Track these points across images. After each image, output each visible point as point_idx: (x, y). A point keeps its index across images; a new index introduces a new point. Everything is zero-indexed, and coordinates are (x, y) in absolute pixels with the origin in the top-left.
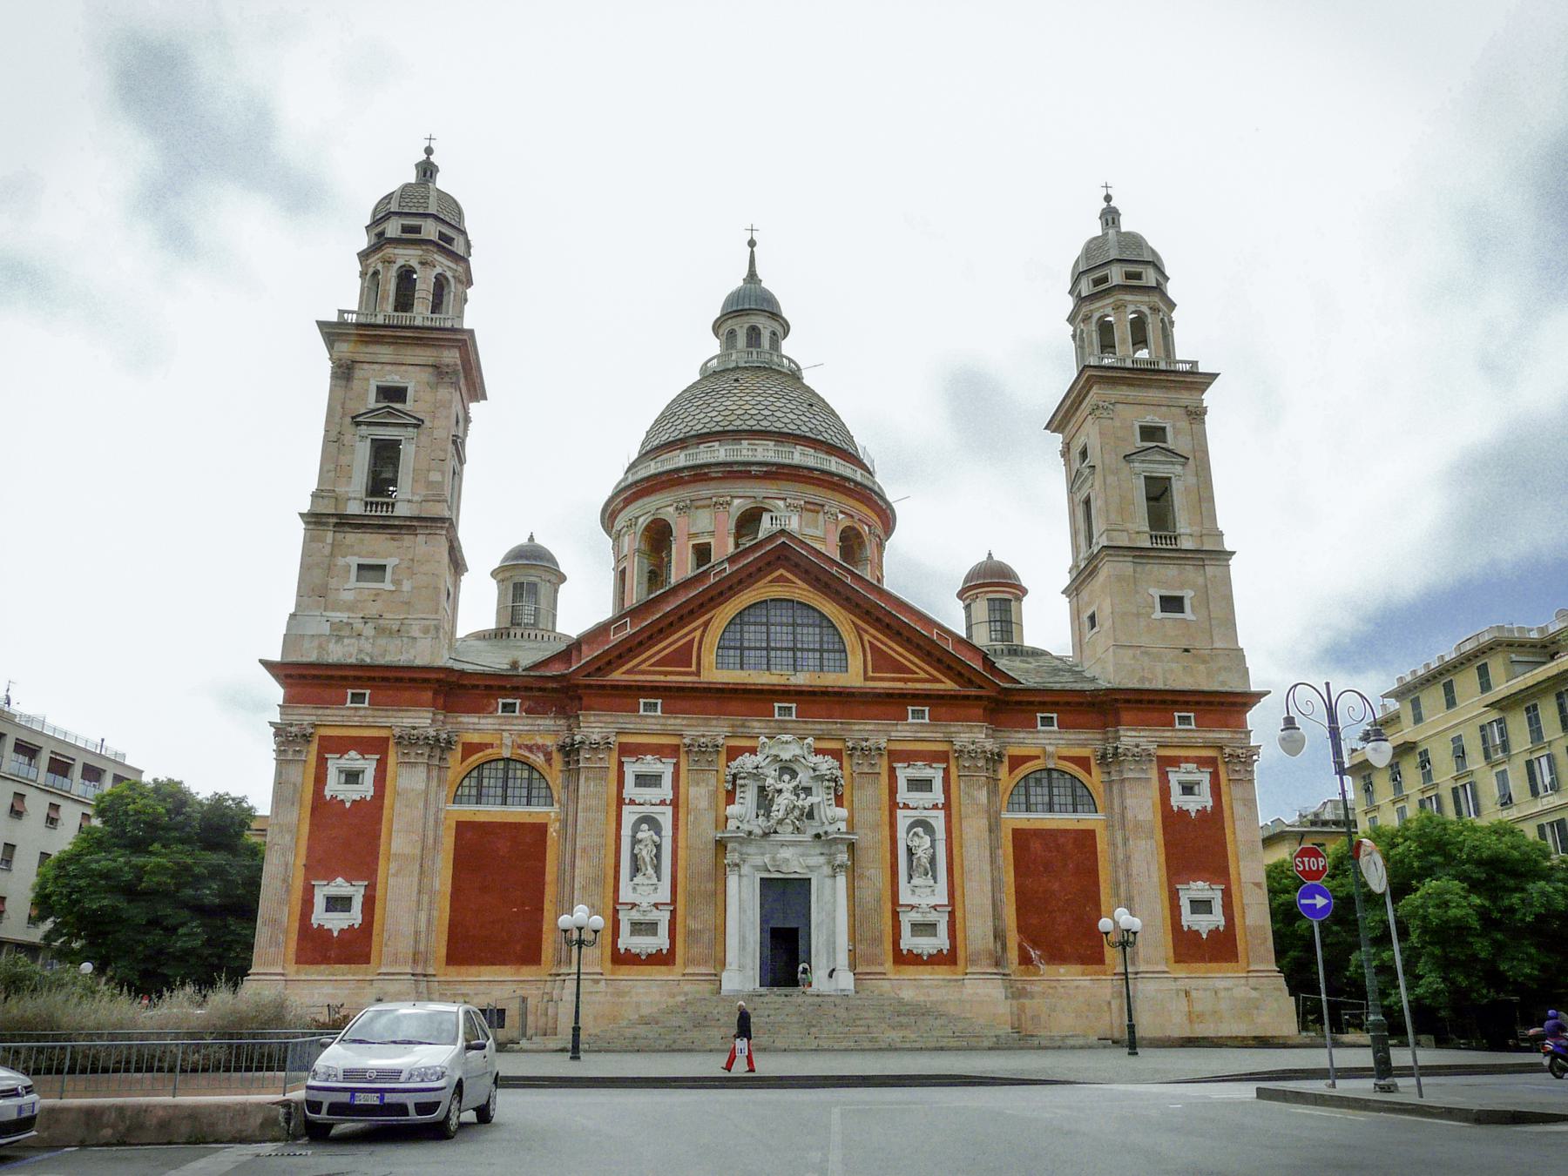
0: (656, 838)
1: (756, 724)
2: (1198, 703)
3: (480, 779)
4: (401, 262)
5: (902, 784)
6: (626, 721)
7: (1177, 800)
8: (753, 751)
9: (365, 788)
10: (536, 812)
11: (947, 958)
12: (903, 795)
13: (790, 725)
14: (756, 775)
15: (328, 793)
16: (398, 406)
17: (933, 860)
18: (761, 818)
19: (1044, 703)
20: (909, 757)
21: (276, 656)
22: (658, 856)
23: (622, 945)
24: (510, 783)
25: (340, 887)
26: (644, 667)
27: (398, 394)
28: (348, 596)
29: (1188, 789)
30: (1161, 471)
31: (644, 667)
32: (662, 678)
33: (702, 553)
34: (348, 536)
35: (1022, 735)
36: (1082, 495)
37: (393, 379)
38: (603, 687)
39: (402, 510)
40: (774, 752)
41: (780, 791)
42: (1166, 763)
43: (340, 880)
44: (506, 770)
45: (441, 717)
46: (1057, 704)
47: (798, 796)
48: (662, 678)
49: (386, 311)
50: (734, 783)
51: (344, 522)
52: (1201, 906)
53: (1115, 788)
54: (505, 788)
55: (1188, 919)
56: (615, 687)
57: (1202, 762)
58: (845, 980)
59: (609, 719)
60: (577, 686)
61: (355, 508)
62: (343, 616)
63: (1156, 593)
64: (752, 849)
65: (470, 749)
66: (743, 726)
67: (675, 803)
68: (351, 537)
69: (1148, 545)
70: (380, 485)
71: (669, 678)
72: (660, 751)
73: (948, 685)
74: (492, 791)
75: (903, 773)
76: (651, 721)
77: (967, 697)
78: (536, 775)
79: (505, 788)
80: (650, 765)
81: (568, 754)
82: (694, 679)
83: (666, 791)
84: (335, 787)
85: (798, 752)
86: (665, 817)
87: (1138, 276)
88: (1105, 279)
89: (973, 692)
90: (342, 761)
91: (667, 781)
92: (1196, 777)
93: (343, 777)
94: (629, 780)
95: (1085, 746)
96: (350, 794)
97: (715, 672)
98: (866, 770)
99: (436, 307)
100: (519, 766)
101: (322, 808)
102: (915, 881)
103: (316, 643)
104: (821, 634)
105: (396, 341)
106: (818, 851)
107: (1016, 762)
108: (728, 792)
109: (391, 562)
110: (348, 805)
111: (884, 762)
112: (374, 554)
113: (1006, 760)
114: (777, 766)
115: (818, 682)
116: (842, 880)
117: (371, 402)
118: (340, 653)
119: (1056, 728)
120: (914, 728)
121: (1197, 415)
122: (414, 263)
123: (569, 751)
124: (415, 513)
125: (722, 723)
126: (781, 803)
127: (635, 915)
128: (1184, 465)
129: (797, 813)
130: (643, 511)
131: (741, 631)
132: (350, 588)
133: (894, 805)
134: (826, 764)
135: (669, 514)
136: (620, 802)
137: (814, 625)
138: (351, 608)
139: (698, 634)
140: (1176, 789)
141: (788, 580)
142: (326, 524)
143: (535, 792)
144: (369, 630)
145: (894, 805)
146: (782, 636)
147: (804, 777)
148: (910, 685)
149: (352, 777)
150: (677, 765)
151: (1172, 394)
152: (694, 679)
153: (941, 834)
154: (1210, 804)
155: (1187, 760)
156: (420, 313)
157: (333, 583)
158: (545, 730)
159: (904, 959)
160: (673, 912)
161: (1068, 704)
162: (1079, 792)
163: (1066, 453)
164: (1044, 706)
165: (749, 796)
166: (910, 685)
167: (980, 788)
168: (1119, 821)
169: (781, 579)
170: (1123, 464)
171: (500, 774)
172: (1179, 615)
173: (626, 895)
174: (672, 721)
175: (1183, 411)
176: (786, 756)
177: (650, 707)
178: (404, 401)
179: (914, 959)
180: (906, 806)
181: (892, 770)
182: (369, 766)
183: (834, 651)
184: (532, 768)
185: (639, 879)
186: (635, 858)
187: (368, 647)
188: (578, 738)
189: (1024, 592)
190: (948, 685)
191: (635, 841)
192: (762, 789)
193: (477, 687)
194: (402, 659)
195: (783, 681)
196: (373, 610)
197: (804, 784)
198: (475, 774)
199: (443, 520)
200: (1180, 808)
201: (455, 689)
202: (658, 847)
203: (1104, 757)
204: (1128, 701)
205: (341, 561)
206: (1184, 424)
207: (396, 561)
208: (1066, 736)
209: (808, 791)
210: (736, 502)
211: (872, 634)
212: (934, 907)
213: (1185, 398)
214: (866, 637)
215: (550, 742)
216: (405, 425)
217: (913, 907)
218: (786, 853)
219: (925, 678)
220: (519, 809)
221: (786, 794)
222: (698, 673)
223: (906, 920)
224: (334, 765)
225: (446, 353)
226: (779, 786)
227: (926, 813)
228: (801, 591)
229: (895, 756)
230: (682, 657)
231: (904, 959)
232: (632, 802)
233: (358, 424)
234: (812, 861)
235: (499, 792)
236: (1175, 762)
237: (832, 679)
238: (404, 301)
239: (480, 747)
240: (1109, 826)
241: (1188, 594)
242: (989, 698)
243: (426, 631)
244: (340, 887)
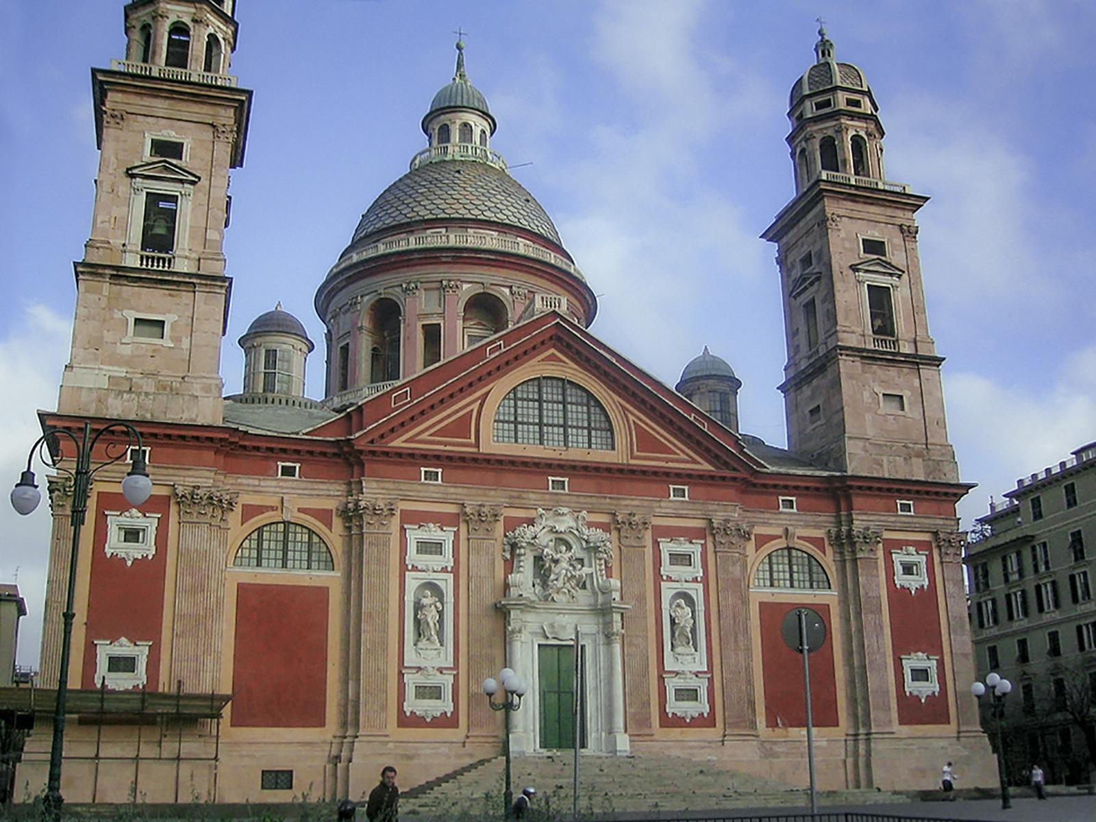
0: (438, 604)
1: (532, 496)
2: (918, 492)
3: (260, 540)
4: (173, 18)
5: (665, 557)
6: (407, 487)
7: (901, 579)
8: (531, 522)
9: (146, 549)
10: (318, 577)
11: (706, 721)
12: (666, 569)
13: (564, 498)
15: (108, 551)
16: (174, 161)
17: (693, 630)
19: (786, 487)
20: (673, 533)
21: (53, 408)
22: (441, 621)
23: (407, 709)
24: (290, 546)
25: (123, 648)
26: (424, 436)
27: (174, 149)
28: (127, 351)
29: (908, 569)
30: (882, 281)
31: (424, 436)
32: (442, 447)
33: (432, 335)
34: (125, 288)
35: (767, 516)
36: (805, 298)
37: (170, 135)
38: (387, 454)
39: (181, 266)
40: (551, 523)
41: (556, 562)
42: (891, 546)
43: (123, 640)
44: (286, 533)
45: (222, 477)
46: (796, 488)
47: (574, 568)
48: (442, 447)
49: (159, 66)
51: (120, 275)
52: (921, 674)
53: (848, 566)
54: (285, 551)
55: (911, 686)
56: (400, 455)
57: (919, 545)
58: (623, 743)
59: (391, 486)
60: (361, 452)
61: (132, 261)
62: (120, 372)
63: (880, 391)
65: (250, 512)
67: (455, 571)
68: (129, 291)
69: (872, 347)
70: (158, 238)
71: (448, 448)
72: (442, 520)
73: (706, 466)
74: (272, 554)
75: (667, 547)
76: (432, 490)
77: (723, 478)
78: (315, 539)
79: (285, 551)
80: (433, 533)
81: (349, 519)
82: (475, 450)
83: (447, 559)
84: (115, 544)
86: (446, 583)
87: (857, 104)
88: (827, 103)
89: (728, 473)
90: (120, 518)
91: (448, 548)
92: (914, 559)
93: (123, 533)
94: (412, 548)
95: (820, 528)
96: (133, 552)
97: (493, 442)
99: (208, 68)
100: (299, 529)
101: (104, 566)
102: (679, 650)
103: (94, 395)
104: (589, 413)
105: (172, 95)
107: (762, 540)
108: (506, 560)
109: (169, 319)
110: (129, 563)
112: (150, 309)
113: (753, 537)
114: (553, 536)
115: (589, 458)
116: (617, 648)
117: (147, 156)
118: (116, 408)
119: (795, 510)
120: (675, 506)
121: (909, 233)
122: (187, 20)
123: (352, 516)
124: (194, 271)
125: (499, 493)
127: (420, 679)
128: (899, 277)
130: (366, 295)
131: (516, 407)
132: (132, 343)
133: (658, 577)
134: (596, 535)
135: (396, 294)
136: (403, 567)
137: (582, 404)
138: (127, 362)
139: (476, 406)
140: (899, 569)
141: (561, 361)
142: (101, 275)
143: (314, 557)
144: (149, 386)
145: (658, 577)
146: (553, 413)
147: (576, 551)
148: (671, 465)
149: (132, 535)
150: (457, 534)
151: (889, 212)
152: (475, 450)
153: (700, 607)
154: (926, 583)
155: (908, 543)
156: (195, 71)
157: (109, 337)
158: (327, 494)
159: (668, 721)
160: (456, 677)
161: (807, 488)
162: (814, 569)
163: (780, 261)
164: (787, 490)
165: (527, 563)
166: (671, 465)
167: (734, 564)
168: (853, 600)
169: (552, 358)
170: (851, 272)
171: (281, 537)
172: (901, 413)
173: (410, 658)
174: (452, 490)
175: (897, 228)
177: (431, 476)
178: (181, 159)
179: (677, 722)
180: (669, 579)
181: (656, 544)
182: (150, 524)
183: (601, 430)
184: (311, 532)
185: (423, 643)
186: (417, 622)
187: (148, 403)
188: (362, 504)
189: (739, 384)
190: (706, 466)
191: (418, 607)
192: (538, 559)
193: (257, 449)
194: (185, 417)
195: (555, 455)
196: (150, 366)
197: (578, 556)
198: (255, 536)
199: (224, 279)
200: (902, 587)
201: (230, 446)
202: (441, 613)
203: (838, 537)
204: (860, 488)
205: (117, 315)
206: (898, 239)
207: (177, 318)
208: (804, 517)
209: (581, 561)
210: (465, 286)
211: (636, 416)
212: (697, 674)
213: (902, 216)
214: (631, 418)
215: (331, 504)
216: (181, 181)
217: (677, 673)
219: (682, 458)
220: (301, 572)
221: (564, 565)
222: (477, 445)
223: (672, 684)
224: (115, 522)
225: (222, 111)
226: (557, 557)
227: (686, 585)
228: (570, 370)
229: (660, 532)
230: (461, 427)
231: (668, 721)
232: (415, 569)
233: (133, 176)
235: (280, 554)
236: (900, 544)
237: (601, 455)
238: (178, 55)
239: (261, 509)
240: (844, 600)
241: (906, 394)
242: (743, 479)
243: (207, 389)
244: (123, 648)
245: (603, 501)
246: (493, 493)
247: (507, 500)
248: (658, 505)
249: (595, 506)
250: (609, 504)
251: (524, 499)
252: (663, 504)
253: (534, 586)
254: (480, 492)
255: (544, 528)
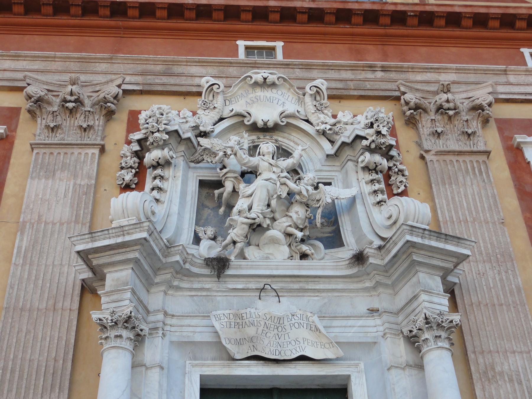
1: (194, 70)
14: (191, 144)
18: (205, 243)
40: (239, 107)
50: (140, 172)
64: (180, 303)
66: (165, 74)
85: (291, 108)
98: (454, 146)
106: (362, 303)
111: (491, 139)
126: (253, 199)
129: (298, 213)
165: (179, 188)
176: (265, 113)
218: (269, 307)
234: (353, 330)
245: (370, 75)
246: (103, 67)
247: (139, 79)
248: (502, 79)
249: (351, 84)
250: (382, 80)
251: (179, 75)
252: (512, 78)
253: (197, 240)
254: (73, 66)
255: (221, 119)
